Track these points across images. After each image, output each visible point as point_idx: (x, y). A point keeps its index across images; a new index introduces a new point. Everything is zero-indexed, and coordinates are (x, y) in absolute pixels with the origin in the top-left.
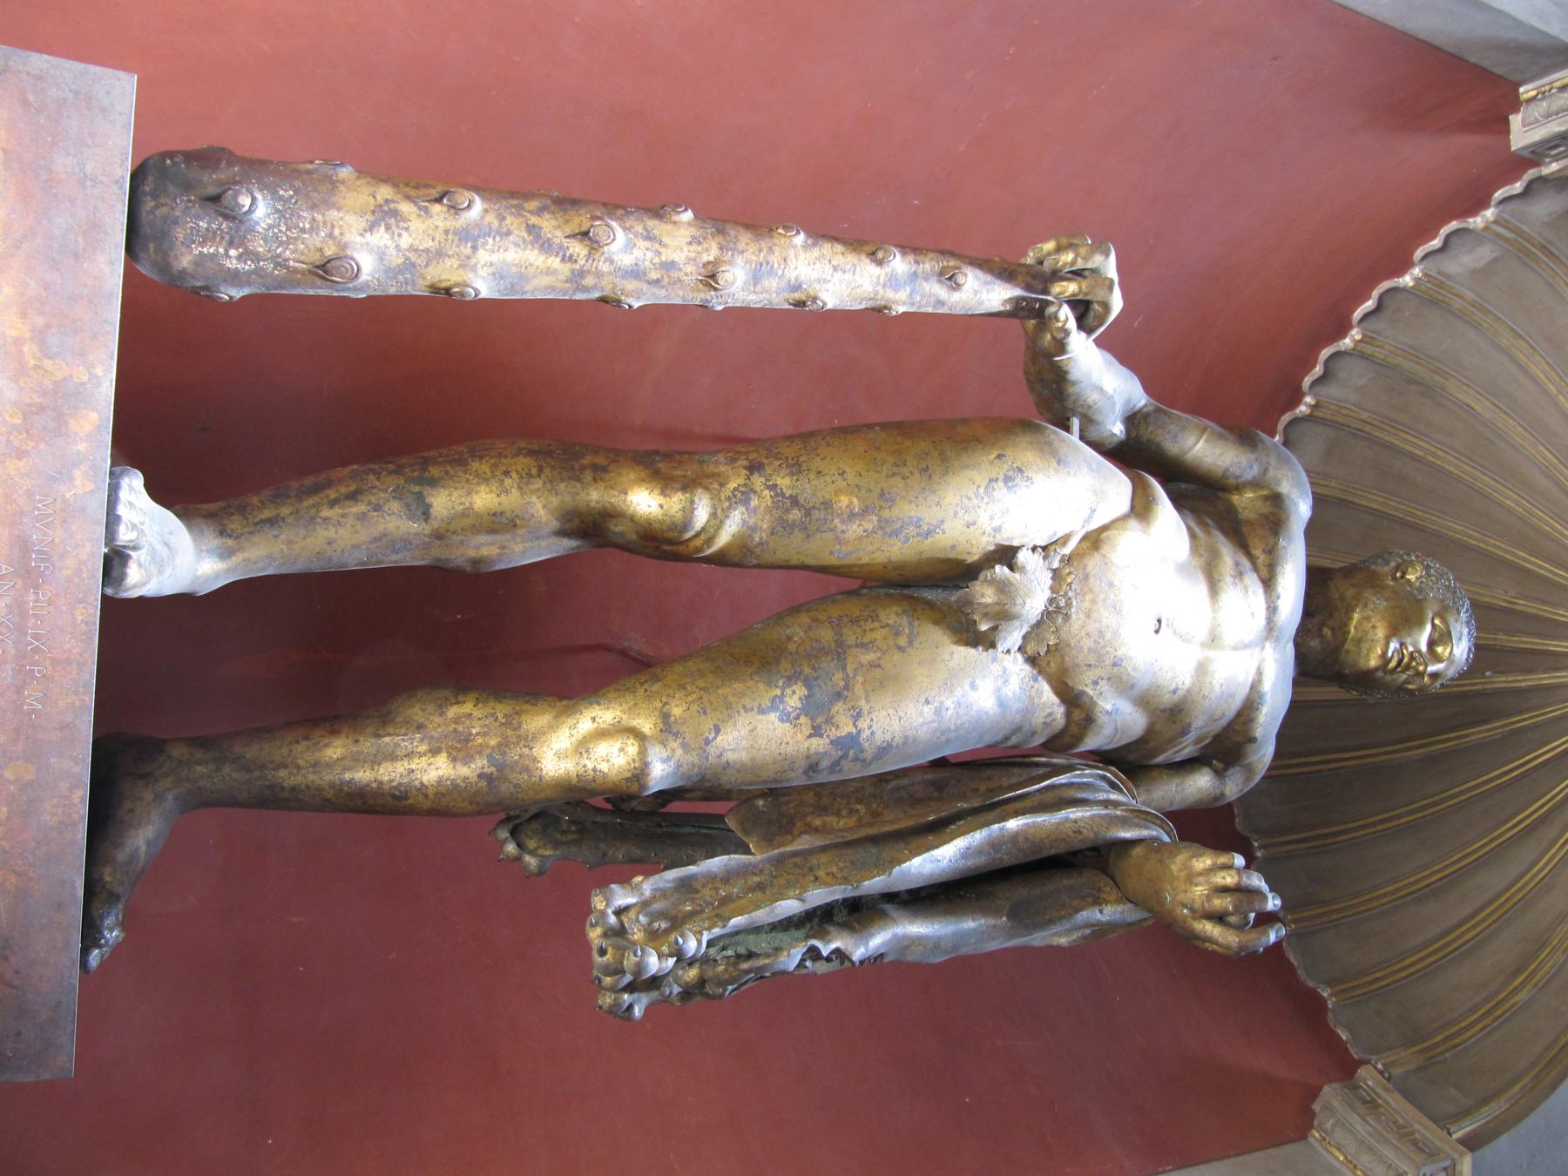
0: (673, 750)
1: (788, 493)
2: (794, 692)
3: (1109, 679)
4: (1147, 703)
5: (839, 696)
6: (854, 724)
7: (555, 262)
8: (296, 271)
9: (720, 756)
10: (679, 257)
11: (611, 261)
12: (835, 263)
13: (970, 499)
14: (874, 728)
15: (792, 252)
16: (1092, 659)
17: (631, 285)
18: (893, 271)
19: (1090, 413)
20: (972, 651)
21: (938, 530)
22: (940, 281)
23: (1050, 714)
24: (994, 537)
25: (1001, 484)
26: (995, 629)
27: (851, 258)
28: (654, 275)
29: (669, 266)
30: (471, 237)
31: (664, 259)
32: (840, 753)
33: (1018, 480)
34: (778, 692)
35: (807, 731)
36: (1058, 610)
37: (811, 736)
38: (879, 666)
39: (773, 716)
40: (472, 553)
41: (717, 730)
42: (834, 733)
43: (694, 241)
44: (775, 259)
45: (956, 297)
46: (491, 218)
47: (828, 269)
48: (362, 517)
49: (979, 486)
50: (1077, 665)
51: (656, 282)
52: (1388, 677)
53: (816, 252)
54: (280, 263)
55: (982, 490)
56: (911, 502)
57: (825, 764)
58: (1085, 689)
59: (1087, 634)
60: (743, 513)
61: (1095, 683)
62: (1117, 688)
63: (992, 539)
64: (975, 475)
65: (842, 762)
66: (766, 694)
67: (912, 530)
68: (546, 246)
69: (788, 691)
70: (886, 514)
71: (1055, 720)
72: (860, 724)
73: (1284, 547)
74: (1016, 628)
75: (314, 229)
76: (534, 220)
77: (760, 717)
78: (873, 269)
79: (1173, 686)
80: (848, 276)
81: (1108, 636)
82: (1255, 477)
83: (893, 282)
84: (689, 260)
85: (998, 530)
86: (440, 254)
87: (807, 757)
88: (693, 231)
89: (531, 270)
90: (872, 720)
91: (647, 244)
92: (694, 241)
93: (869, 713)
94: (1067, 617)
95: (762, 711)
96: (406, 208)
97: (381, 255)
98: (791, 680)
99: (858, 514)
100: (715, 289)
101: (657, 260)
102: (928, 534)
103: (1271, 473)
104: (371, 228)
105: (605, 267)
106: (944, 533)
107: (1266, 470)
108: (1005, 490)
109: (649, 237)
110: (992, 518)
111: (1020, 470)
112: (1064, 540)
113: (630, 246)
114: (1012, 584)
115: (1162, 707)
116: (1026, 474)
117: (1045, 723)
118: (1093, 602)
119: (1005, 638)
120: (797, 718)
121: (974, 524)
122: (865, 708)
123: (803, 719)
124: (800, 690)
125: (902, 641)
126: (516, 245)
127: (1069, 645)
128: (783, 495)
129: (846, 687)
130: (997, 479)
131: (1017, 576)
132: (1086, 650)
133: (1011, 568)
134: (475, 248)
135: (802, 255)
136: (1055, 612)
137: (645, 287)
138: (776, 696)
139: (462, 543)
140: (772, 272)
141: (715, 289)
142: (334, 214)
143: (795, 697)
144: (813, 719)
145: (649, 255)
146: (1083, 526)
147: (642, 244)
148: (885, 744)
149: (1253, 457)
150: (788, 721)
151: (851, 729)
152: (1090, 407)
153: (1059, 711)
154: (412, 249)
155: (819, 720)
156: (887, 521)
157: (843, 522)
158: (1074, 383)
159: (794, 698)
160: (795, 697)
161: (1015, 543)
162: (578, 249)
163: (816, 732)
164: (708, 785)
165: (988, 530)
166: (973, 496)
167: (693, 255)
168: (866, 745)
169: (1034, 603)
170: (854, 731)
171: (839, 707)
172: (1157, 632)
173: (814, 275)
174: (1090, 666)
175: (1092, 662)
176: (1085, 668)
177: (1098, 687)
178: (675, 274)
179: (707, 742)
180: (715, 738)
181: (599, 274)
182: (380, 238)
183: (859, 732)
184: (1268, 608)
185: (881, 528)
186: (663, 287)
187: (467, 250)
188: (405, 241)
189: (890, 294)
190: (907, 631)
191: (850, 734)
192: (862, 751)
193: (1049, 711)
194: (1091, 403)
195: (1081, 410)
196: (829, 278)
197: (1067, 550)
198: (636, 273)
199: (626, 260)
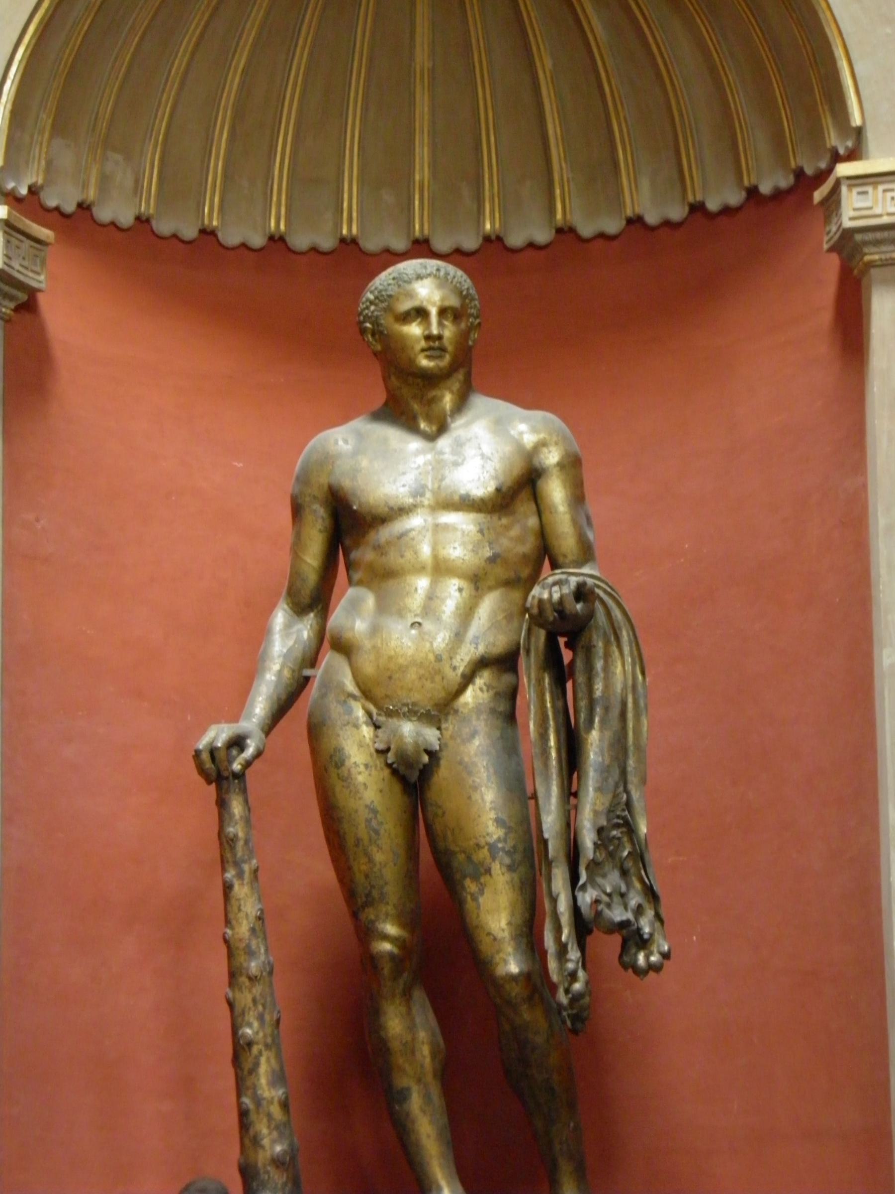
0: (500, 958)
1: (364, 899)
2: (469, 887)
3: (451, 658)
4: (471, 609)
5: (469, 858)
6: (483, 847)
7: (263, 1060)
8: (288, 1177)
9: (503, 930)
10: (249, 998)
11: (257, 1033)
12: (237, 911)
13: (351, 792)
14: (485, 834)
15: (236, 936)
16: (438, 678)
17: (267, 1017)
18: (234, 876)
19: (296, 668)
20: (443, 763)
21: (372, 806)
22: (234, 847)
23: (481, 689)
24: (371, 767)
25: (340, 771)
26: (427, 752)
27: (233, 901)
28: (260, 1008)
29: (254, 1001)
30: (258, 1101)
31: (251, 1005)
32: (501, 853)
33: (337, 759)
34: (469, 897)
35: (488, 876)
36: (409, 711)
37: (490, 875)
38: (453, 830)
39: (481, 900)
40: (428, 1060)
41: (489, 934)
42: (489, 860)
43: (240, 989)
44: (242, 945)
45: (241, 834)
46: (249, 1092)
47: (241, 915)
48: (413, 1122)
49: (343, 786)
50: (444, 687)
51: (264, 1006)
52: (450, 348)
53: (234, 922)
54: (285, 1184)
55: (345, 784)
56: (357, 828)
57: (507, 861)
58: (459, 674)
59: (423, 687)
60: (379, 923)
61: (455, 668)
62: (458, 648)
63: (373, 768)
64: (338, 789)
65: (507, 849)
66: (470, 905)
67: (374, 823)
68: (257, 1064)
69: (468, 890)
70: (366, 841)
71: (485, 684)
72: (482, 842)
73: (360, 505)
74: (424, 738)
75: (268, 1173)
76: (246, 1072)
77: (482, 908)
78: (236, 887)
79: (457, 594)
80: (242, 902)
81: (422, 672)
82: (321, 506)
83: (240, 875)
84: (250, 991)
85: (366, 766)
86: (269, 1116)
87: (503, 874)
88: (236, 990)
89: (269, 1069)
90: (480, 836)
91: (246, 1014)
92: (240, 989)
93: (476, 838)
94: (414, 704)
95: (478, 907)
96: (252, 1132)
97: (274, 1142)
98: (463, 887)
99: (369, 859)
100: (262, 973)
101: (253, 1009)
102: (375, 812)
103: (316, 493)
104: (263, 1147)
105: (261, 1034)
106: (373, 802)
107: (315, 497)
108: (343, 768)
109: (243, 1013)
110: (360, 773)
111: (331, 757)
112: (369, 714)
113: (250, 1025)
114: (397, 751)
115: (473, 593)
116: (333, 753)
117: (488, 691)
118: (402, 688)
119: (431, 745)
120: (481, 884)
121: (365, 784)
122: (475, 841)
123: (482, 880)
124: (468, 882)
125: (440, 812)
126: (258, 1080)
127: (431, 698)
128: (366, 902)
129: (464, 852)
130: (338, 775)
131: (392, 747)
132: (433, 685)
133: (388, 750)
134: (264, 1099)
135: (237, 930)
136: (413, 713)
137: (267, 1011)
138: (471, 898)
139: (422, 1066)
140: (248, 946)
141: (262, 973)
142: (260, 1164)
143: (471, 885)
144: (481, 874)
145: (251, 1013)
146: (359, 701)
147: (246, 1018)
148: (495, 824)
149: (307, 510)
150: (483, 890)
151: (485, 851)
152: (293, 671)
153: (479, 682)
154: (269, 1127)
155: (482, 870)
156: (370, 840)
157: (375, 865)
158: (279, 699)
159: (471, 886)
160: (471, 885)
161: (373, 751)
162: (255, 1050)
163: (488, 871)
164: (524, 929)
165: (367, 773)
166: (349, 790)
167: (247, 990)
168: (495, 837)
169: (408, 729)
170: (486, 848)
171: (475, 858)
172: (420, 624)
173: (245, 922)
174: (443, 678)
175: (441, 678)
176: (445, 681)
177: (458, 664)
178: (258, 997)
179: (495, 939)
180: (493, 935)
181: (265, 1036)
182: (266, 1142)
183: (487, 844)
184: (400, 515)
185: (375, 842)
186: (266, 1001)
187: (264, 1103)
188: (265, 1131)
189: (247, 875)
190: (434, 808)
191: (490, 850)
192: (499, 840)
193: (478, 690)
194: (291, 672)
195: (297, 672)
196: (245, 913)
197: (374, 711)
198: (261, 1018)
199: (256, 1024)
